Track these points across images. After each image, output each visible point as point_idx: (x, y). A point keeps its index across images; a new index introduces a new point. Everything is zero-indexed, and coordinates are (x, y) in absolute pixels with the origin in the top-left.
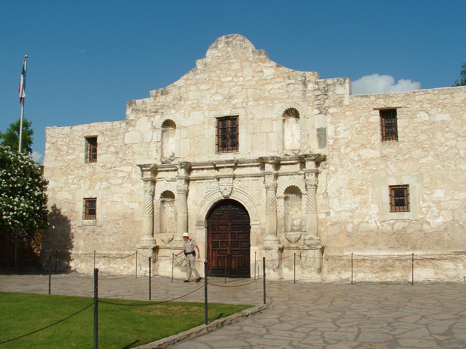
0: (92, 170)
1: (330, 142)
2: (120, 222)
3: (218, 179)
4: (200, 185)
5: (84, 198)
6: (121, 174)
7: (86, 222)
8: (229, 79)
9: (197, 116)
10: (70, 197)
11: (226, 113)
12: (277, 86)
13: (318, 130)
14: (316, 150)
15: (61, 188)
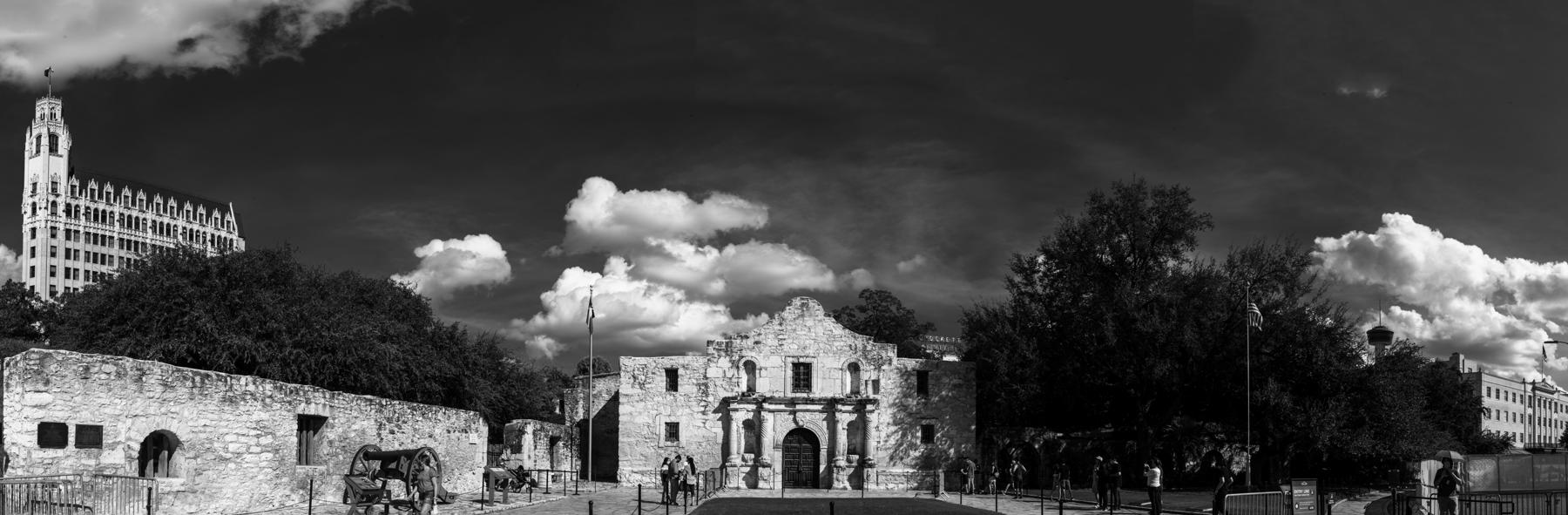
0: (672, 397)
1: (882, 390)
2: (704, 444)
3: (794, 413)
4: (779, 416)
5: (666, 423)
6: (703, 403)
7: (669, 443)
8: (804, 333)
9: (776, 360)
10: (651, 422)
11: (801, 360)
12: (842, 343)
13: (873, 381)
14: (872, 396)
15: (640, 413)
